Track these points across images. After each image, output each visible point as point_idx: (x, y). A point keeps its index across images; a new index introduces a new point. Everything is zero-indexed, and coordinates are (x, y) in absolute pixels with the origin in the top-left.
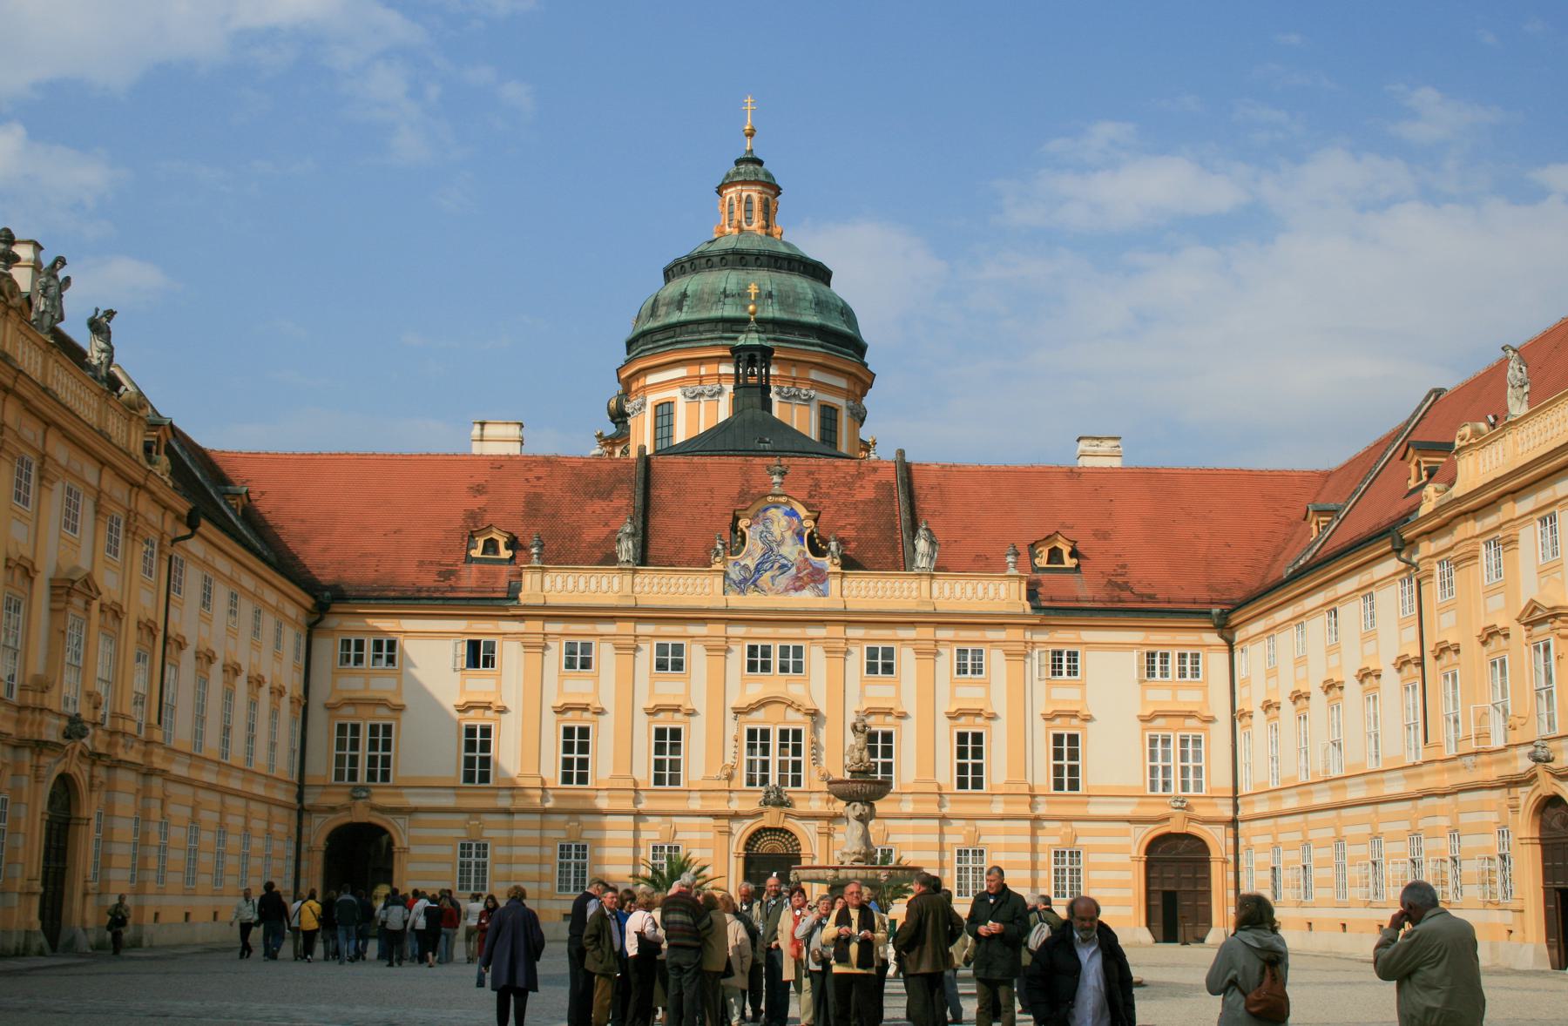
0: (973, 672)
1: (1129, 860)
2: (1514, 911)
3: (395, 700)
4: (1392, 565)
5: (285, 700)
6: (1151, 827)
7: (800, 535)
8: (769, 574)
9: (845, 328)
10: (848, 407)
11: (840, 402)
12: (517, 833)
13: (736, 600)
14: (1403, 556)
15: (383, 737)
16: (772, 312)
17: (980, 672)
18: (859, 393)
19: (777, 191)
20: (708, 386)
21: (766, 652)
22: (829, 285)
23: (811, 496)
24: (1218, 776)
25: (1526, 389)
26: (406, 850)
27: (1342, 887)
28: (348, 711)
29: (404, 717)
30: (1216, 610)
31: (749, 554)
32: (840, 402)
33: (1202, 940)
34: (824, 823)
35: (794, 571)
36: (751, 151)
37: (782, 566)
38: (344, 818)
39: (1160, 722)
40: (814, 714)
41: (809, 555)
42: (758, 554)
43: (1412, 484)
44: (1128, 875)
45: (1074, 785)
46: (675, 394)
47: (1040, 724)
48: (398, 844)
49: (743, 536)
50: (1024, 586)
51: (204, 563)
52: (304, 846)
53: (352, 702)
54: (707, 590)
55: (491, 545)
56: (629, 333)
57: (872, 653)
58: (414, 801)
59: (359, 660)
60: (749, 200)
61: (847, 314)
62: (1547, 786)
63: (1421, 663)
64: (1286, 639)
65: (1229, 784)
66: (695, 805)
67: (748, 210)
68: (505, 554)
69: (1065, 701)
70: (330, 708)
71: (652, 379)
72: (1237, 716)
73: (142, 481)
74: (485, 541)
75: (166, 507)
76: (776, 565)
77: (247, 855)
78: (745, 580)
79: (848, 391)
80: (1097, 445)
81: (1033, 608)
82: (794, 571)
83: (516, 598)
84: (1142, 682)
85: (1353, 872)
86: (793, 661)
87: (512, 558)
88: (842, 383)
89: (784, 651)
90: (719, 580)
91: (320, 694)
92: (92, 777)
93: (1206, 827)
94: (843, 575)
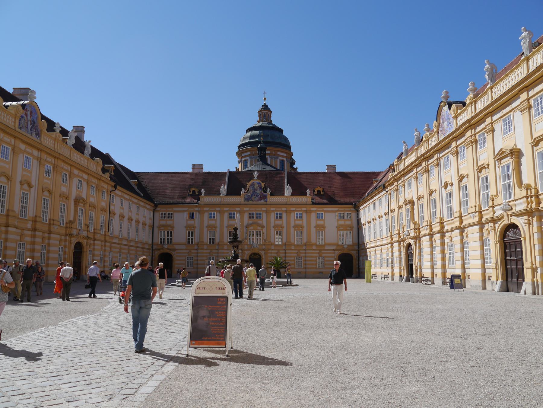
0: (300, 218)
5: (147, 227)
7: (261, 188)
8: (254, 197)
9: (285, 143)
11: (285, 159)
15: (170, 234)
16: (269, 139)
19: (271, 112)
21: (253, 214)
23: (265, 180)
31: (250, 193)
32: (285, 159)
36: (265, 104)
38: (162, 251)
41: (263, 192)
42: (251, 192)
46: (248, 158)
49: (248, 188)
51: (121, 196)
52: (153, 258)
56: (238, 145)
57: (277, 214)
58: (177, 247)
59: (165, 217)
61: (286, 139)
63: (388, 213)
68: (197, 193)
71: (243, 155)
73: (100, 178)
75: (108, 184)
78: (249, 198)
79: (287, 157)
82: (259, 196)
86: (259, 216)
88: (285, 155)
89: (257, 214)
91: (156, 224)
92: (87, 243)
93: (352, 252)
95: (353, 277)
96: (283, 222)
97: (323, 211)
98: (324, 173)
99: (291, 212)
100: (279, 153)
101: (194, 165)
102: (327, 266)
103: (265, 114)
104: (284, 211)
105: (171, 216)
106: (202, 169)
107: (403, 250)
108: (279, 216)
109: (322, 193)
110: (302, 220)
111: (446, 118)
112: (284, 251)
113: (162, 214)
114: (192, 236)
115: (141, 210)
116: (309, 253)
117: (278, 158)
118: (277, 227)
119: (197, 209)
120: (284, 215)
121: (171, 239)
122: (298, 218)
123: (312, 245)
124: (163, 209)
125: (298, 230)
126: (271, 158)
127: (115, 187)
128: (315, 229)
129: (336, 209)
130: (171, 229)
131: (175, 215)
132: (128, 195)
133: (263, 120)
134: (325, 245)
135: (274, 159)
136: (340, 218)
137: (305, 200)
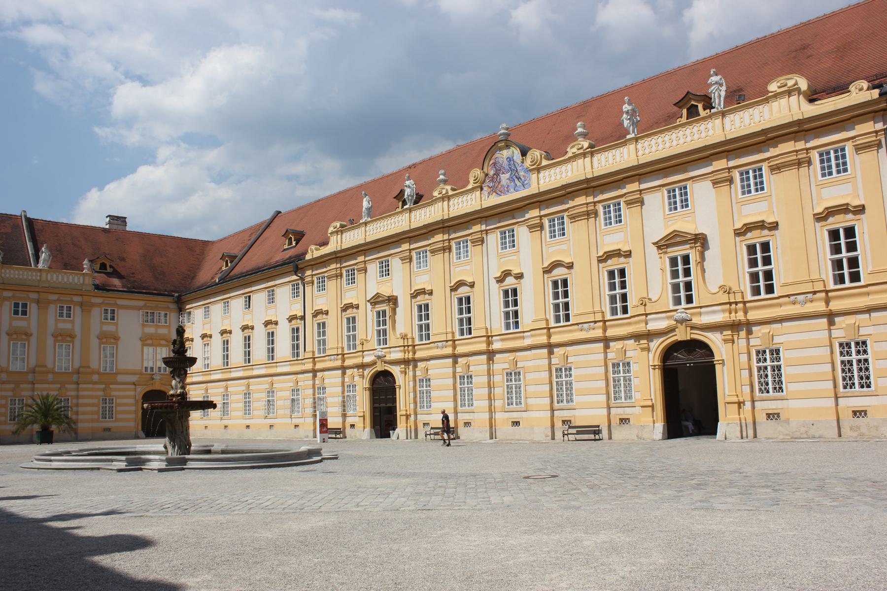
2: (359, 417)
17: (70, 317)
30: (176, 295)
47: (97, 341)
57: (16, 305)
62: (380, 367)
63: (303, 318)
80: (116, 220)
84: (143, 325)
96: (29, 324)
97: (116, 305)
98: (104, 230)
99: (50, 302)
102: (120, 416)
104: (32, 301)
108: (20, 310)
109: (109, 270)
110: (73, 322)
111: (507, 167)
112: (30, 386)
116: (84, 390)
118: (16, 333)
120: (33, 309)
122: (62, 316)
123: (93, 373)
125: (62, 341)
128: (98, 340)
129: (141, 303)
134: (117, 374)
137: (79, 280)
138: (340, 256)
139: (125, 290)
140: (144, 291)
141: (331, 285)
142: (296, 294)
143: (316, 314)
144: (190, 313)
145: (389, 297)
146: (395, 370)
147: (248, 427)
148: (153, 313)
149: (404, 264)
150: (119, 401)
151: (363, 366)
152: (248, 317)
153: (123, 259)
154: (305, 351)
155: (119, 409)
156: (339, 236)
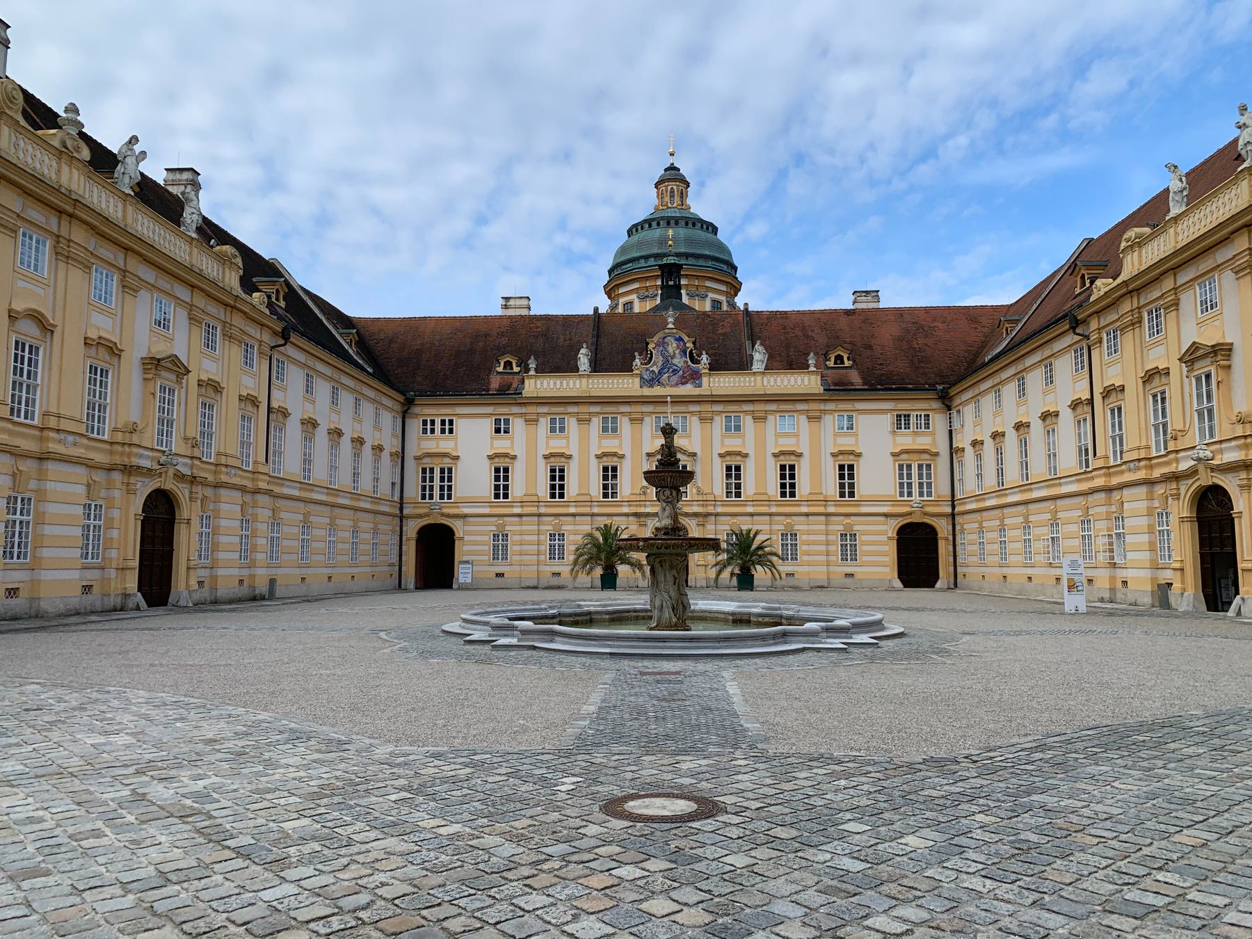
1: (886, 539)
2: (1174, 569)
3: (454, 454)
4: (1070, 339)
5: (386, 456)
6: (900, 519)
10: (727, 302)
11: (723, 298)
12: (525, 528)
13: (647, 391)
14: (1078, 331)
15: (447, 474)
18: (733, 293)
19: (688, 185)
20: (651, 292)
22: (716, 234)
24: (941, 486)
25: (1185, 193)
26: (461, 539)
27: (1028, 553)
28: (426, 460)
29: (459, 463)
30: (940, 387)
31: (655, 364)
32: (723, 298)
33: (933, 587)
34: (701, 519)
35: (681, 373)
37: (675, 370)
39: (904, 456)
40: (694, 455)
41: (690, 363)
42: (660, 364)
43: (1078, 291)
44: (886, 548)
45: (852, 494)
46: (634, 297)
47: (830, 460)
48: (457, 535)
50: (819, 377)
52: (404, 538)
53: (430, 455)
54: (630, 386)
55: (508, 364)
56: (609, 268)
58: (466, 511)
59: (433, 431)
60: (672, 191)
62: (1205, 479)
63: (1091, 402)
64: (988, 401)
65: (947, 492)
66: (626, 510)
67: (672, 196)
68: (516, 369)
69: (845, 445)
70: (417, 458)
71: (621, 290)
72: (954, 451)
74: (505, 362)
76: (671, 370)
77: (356, 543)
81: (825, 390)
82: (681, 373)
83: (521, 393)
85: (1038, 546)
87: (520, 372)
88: (723, 288)
90: (637, 380)
91: (411, 452)
92: (191, 493)
93: (934, 519)
94: (710, 374)
95: (938, 585)
98: (848, 313)
100: (708, 284)
101: (507, 299)
102: (865, 558)
103: (672, 191)
105: (448, 427)
106: (529, 309)
107: (1181, 509)
113: (425, 423)
114: (506, 478)
115: (368, 409)
117: (707, 296)
119: (516, 410)
121: (450, 488)
124: (427, 411)
126: (690, 296)
127: (285, 336)
130: (451, 461)
131: (459, 424)
132: (329, 364)
133: (670, 205)
135: (697, 298)
136: (901, 428)
138: (1134, 288)
139: (866, 387)
140: (894, 387)
141: (1128, 342)
142: (1078, 368)
143: (1107, 393)
144: (959, 411)
145: (1213, 346)
146: (1230, 483)
147: (1030, 578)
148: (909, 416)
149: (1241, 280)
150: (864, 538)
151: (1176, 477)
152: (1023, 409)
153: (869, 347)
154: (1095, 455)
155: (865, 548)
156: (1136, 254)
